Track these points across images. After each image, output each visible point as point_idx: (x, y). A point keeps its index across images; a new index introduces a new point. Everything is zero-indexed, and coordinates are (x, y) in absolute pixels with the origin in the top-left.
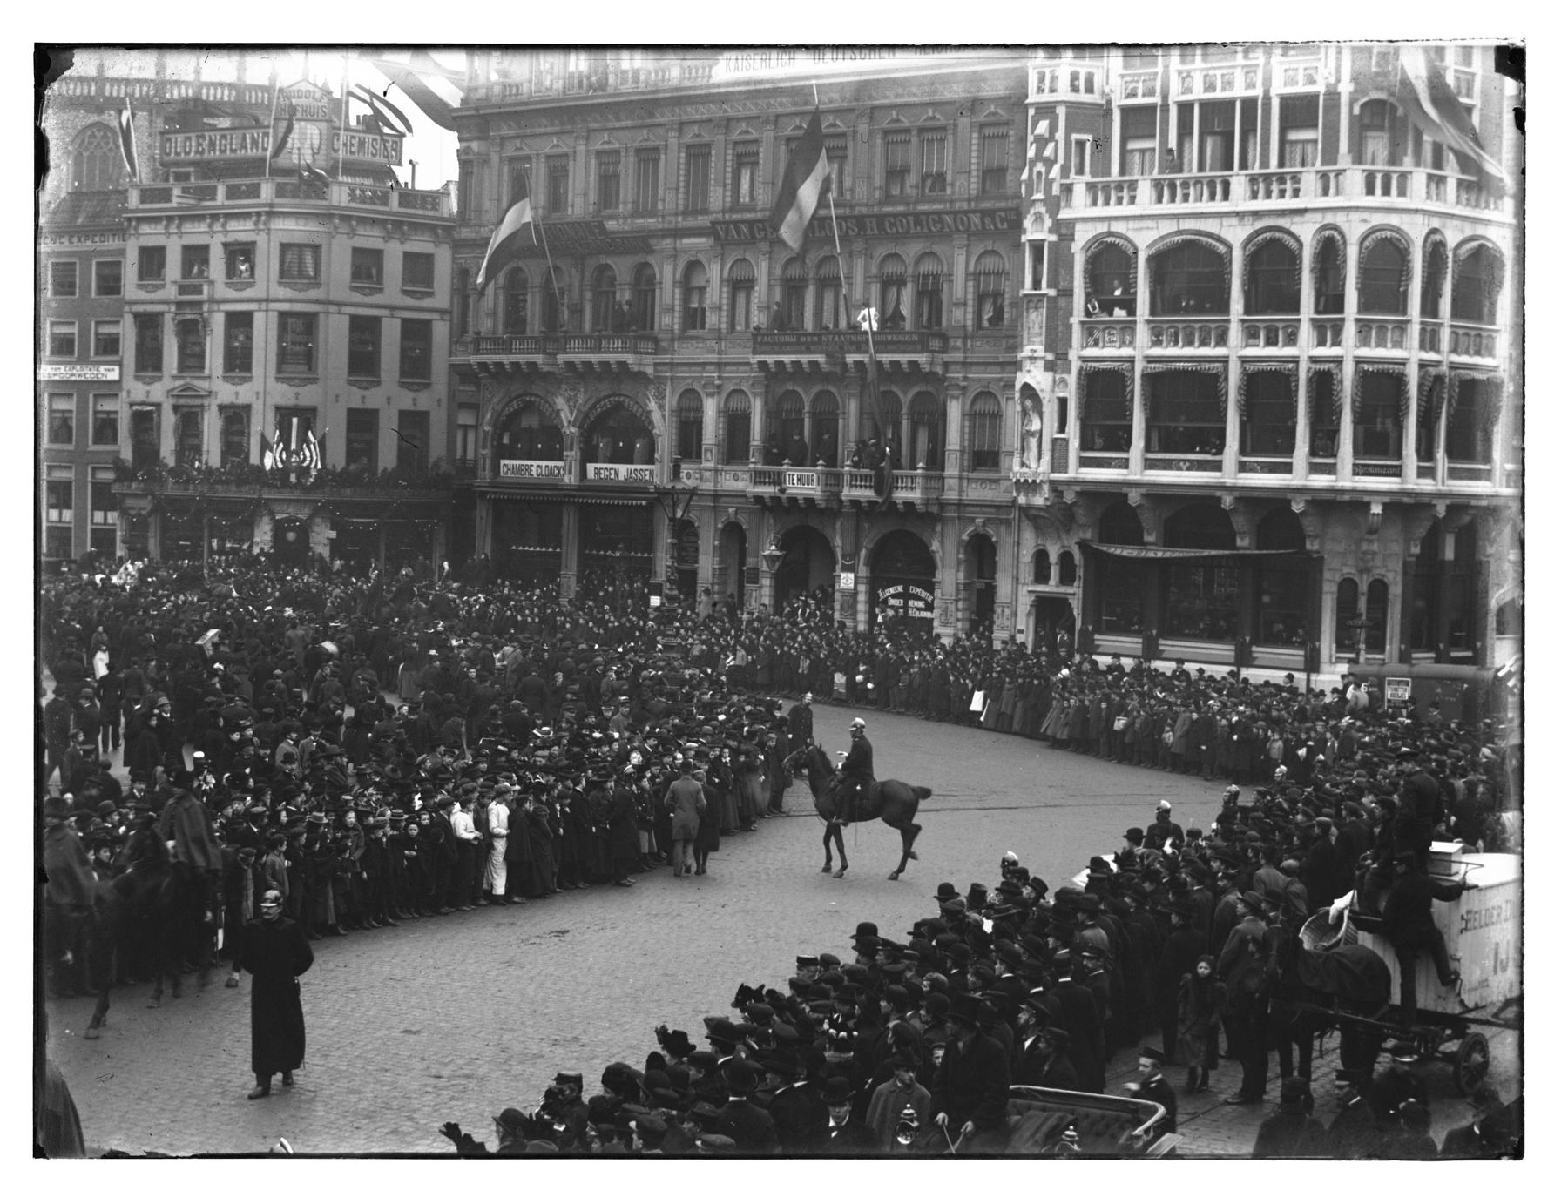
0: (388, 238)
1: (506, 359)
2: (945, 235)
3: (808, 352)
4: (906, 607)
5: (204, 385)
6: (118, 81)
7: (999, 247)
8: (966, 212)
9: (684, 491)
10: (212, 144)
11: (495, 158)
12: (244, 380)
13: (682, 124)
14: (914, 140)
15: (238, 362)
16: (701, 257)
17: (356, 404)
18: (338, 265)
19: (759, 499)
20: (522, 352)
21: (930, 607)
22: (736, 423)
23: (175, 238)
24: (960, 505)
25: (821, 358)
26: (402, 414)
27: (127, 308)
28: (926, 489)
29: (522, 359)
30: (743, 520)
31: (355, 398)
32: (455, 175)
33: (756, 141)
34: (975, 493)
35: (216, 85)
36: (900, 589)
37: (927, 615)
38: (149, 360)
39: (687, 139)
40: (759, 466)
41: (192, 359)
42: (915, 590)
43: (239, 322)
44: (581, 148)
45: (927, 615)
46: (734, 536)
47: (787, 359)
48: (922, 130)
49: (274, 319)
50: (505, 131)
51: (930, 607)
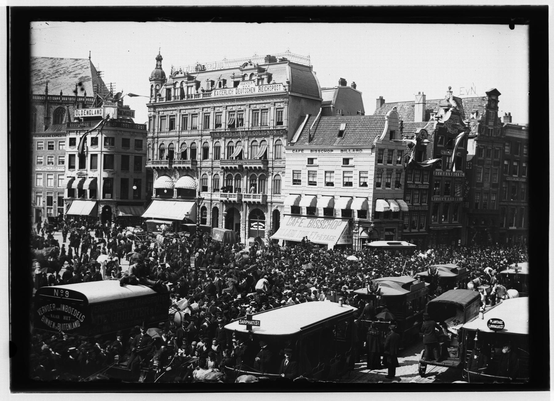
0: (132, 135)
1: (160, 166)
2: (267, 136)
3: (234, 164)
4: (258, 228)
5: (85, 172)
6: (66, 97)
7: (281, 139)
8: (273, 130)
9: (201, 199)
10: (87, 112)
11: (157, 116)
12: (95, 171)
13: (215, 107)
14: (260, 112)
15: (93, 167)
16: (208, 141)
17: (123, 177)
18: (118, 143)
19: (222, 201)
20: (164, 164)
21: (264, 228)
22: (216, 181)
24: (272, 203)
25: (237, 166)
26: (134, 179)
28: (262, 199)
29: (164, 166)
30: (218, 206)
31: (123, 175)
32: (148, 120)
33: (221, 112)
34: (274, 199)
35: (90, 98)
36: (256, 223)
37: (263, 229)
38: (71, 167)
39: (204, 112)
40: (222, 193)
41: (82, 165)
42: (260, 223)
43: (94, 156)
44: (178, 114)
45: (263, 229)
46: (215, 211)
47: (229, 166)
48: (262, 110)
49: (103, 156)
50: (160, 109)
51: (264, 228)
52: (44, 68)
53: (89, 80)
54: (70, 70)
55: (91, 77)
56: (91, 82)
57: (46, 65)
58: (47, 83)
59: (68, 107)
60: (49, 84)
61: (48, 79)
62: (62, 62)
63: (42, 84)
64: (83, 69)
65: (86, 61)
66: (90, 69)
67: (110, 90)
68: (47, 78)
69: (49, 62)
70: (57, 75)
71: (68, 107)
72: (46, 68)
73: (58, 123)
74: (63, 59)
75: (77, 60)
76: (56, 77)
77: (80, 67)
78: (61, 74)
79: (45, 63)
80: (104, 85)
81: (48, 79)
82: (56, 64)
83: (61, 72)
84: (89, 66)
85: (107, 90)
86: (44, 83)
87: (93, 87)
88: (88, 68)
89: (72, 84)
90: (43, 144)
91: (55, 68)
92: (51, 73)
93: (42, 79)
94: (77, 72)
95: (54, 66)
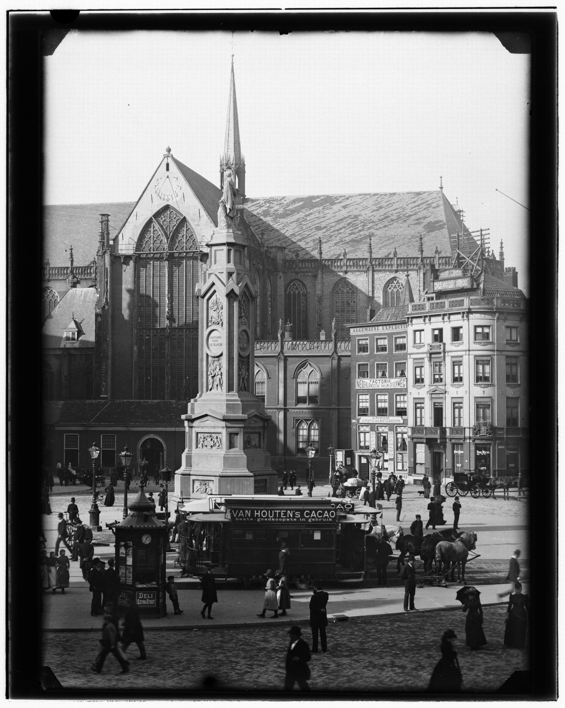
12: (460, 386)
23: (428, 325)
27: (409, 356)
52: (363, 213)
53: (441, 227)
54: (408, 211)
55: (445, 221)
56: (445, 231)
57: (367, 207)
58: (370, 236)
59: (408, 276)
60: (373, 238)
61: (372, 231)
62: (395, 199)
63: (361, 239)
64: (431, 209)
65: (434, 195)
66: (442, 207)
67: (479, 242)
68: (370, 228)
69: (370, 202)
70: (386, 222)
71: (408, 276)
72: (366, 212)
73: (392, 305)
74: (394, 194)
75: (418, 194)
76: (385, 226)
77: (424, 206)
78: (392, 220)
79: (365, 203)
80: (470, 234)
81: (372, 231)
82: (384, 204)
83: (392, 217)
84: (441, 202)
85: (475, 242)
86: (366, 237)
87: (451, 238)
88: (438, 206)
89: (413, 237)
90: (368, 341)
91: (382, 212)
92: (375, 219)
93: (360, 231)
94: (420, 215)
95: (381, 207)
